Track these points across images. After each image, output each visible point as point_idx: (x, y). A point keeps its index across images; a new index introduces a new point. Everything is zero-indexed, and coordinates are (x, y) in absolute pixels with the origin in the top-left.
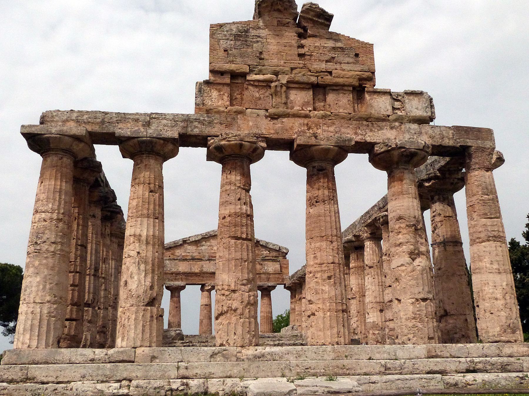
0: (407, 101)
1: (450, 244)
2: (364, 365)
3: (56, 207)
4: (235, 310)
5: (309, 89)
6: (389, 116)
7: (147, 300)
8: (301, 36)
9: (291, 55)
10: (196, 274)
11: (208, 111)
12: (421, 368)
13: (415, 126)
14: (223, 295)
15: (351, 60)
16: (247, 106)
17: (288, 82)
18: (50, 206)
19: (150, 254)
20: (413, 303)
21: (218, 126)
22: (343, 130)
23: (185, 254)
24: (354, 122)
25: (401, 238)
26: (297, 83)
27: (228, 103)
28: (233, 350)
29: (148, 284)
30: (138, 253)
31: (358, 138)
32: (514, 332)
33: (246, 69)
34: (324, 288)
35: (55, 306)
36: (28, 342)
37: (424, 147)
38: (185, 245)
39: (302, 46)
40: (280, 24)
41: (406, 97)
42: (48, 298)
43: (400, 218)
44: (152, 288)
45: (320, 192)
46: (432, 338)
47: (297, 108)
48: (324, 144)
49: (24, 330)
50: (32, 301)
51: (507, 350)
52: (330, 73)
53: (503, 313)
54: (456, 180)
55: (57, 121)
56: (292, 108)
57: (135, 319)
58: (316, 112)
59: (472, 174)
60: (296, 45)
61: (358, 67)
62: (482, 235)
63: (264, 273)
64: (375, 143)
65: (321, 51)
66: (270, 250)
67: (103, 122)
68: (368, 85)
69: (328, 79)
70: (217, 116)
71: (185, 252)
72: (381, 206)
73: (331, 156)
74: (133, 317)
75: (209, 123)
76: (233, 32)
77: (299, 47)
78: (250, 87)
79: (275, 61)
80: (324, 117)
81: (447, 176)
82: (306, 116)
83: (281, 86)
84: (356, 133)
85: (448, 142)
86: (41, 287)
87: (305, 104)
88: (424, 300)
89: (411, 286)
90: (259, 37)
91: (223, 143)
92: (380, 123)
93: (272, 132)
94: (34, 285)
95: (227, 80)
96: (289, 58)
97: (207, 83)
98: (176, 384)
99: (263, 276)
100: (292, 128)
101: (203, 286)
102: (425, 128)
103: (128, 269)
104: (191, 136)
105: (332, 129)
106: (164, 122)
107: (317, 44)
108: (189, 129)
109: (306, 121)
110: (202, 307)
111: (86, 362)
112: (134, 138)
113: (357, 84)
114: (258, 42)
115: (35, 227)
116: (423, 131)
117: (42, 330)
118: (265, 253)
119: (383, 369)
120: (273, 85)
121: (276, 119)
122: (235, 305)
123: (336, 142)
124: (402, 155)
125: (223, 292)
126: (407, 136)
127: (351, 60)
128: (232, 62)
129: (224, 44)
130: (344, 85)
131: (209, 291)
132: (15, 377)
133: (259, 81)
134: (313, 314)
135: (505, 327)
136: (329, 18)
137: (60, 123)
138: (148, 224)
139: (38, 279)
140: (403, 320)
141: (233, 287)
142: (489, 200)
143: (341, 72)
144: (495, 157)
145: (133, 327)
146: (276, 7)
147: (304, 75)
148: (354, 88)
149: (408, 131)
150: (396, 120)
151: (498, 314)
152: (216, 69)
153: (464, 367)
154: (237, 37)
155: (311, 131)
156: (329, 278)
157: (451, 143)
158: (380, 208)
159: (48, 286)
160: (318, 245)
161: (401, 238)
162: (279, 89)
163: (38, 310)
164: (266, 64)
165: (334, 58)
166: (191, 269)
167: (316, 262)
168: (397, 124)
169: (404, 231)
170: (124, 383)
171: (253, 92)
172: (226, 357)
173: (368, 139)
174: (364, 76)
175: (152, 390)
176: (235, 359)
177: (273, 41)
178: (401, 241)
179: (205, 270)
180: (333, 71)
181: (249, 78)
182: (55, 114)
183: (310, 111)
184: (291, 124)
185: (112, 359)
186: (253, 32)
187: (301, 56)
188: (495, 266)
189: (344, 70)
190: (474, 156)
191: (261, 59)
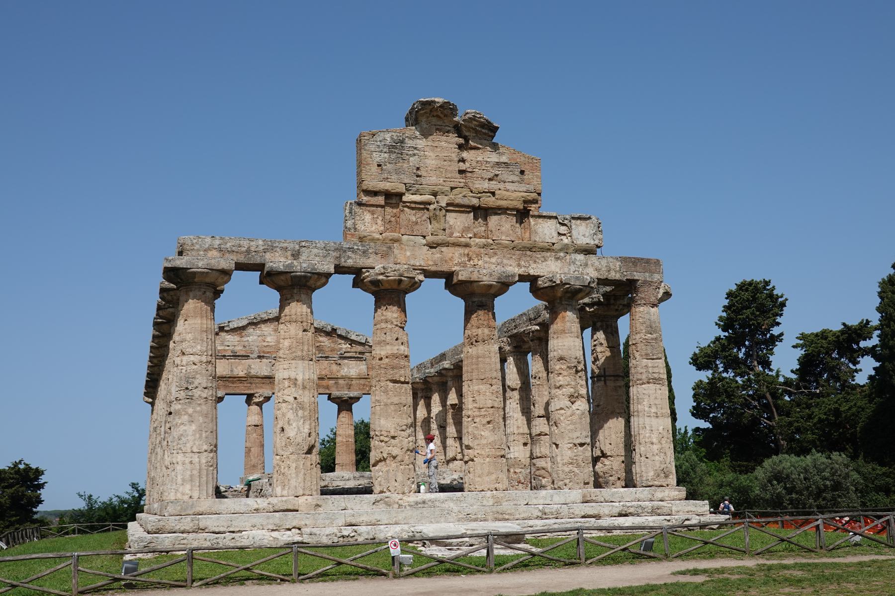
0: (573, 227)
1: (612, 378)
2: (523, 511)
3: (205, 349)
4: (394, 458)
5: (469, 212)
6: (553, 244)
7: (306, 448)
8: (461, 147)
9: (451, 172)
10: (239, 379)
11: (361, 239)
12: (576, 513)
13: (580, 257)
14: (382, 441)
15: (516, 178)
16: (403, 231)
17: (448, 205)
18: (199, 347)
19: (306, 400)
20: (570, 448)
21: (373, 256)
22: (505, 261)
23: (222, 348)
24: (518, 252)
25: (561, 380)
26: (458, 205)
27: (382, 228)
28: (395, 497)
29: (307, 431)
30: (295, 398)
31: (521, 271)
32: (666, 477)
33: (401, 188)
34: (483, 433)
35: (211, 455)
36: (188, 492)
37: (589, 283)
38: (223, 334)
39: (463, 160)
41: (573, 221)
42: (205, 447)
43: (561, 359)
45: (480, 331)
46: (588, 483)
47: (456, 234)
48: (486, 280)
49: (183, 480)
50: (189, 451)
51: (659, 494)
52: (493, 194)
53: (657, 458)
54: (621, 307)
55: (198, 250)
56: (451, 235)
57: (296, 468)
58: (477, 240)
59: (637, 310)
60: (456, 159)
61: (523, 188)
62: (644, 377)
63: (343, 378)
64: (539, 277)
65: (483, 167)
66: (352, 342)
67: (248, 251)
68: (533, 207)
69: (490, 201)
70: (372, 244)
71: (222, 344)
72: (532, 316)
73: (492, 291)
74: (294, 465)
75: (364, 252)
76: (388, 143)
77: (459, 161)
78: (406, 209)
79: (433, 179)
80: (484, 246)
81: (612, 301)
82: (467, 245)
83: (440, 210)
84: (519, 265)
85: (614, 276)
86: (198, 435)
87: (467, 229)
88: (582, 445)
89: (571, 431)
90: (416, 148)
91: (381, 277)
92: (544, 254)
93: (431, 263)
94: (191, 433)
95: (381, 200)
96: (449, 175)
98: (347, 531)
99: (341, 382)
100: (451, 259)
101: (249, 398)
103: (284, 415)
104: (343, 267)
105: (493, 260)
106: (315, 251)
107: (479, 159)
108: (343, 260)
109: (466, 251)
110: (249, 428)
111: (251, 512)
112: (287, 272)
113: (522, 207)
114: (414, 155)
115: (184, 371)
116: (589, 263)
117: (202, 480)
118: (345, 346)
119: (540, 514)
120: (432, 207)
121: (435, 248)
122: (395, 451)
123: (499, 278)
124: (567, 291)
125: (382, 438)
127: (516, 178)
129: (377, 157)
130: (508, 209)
131: (260, 404)
132: (187, 528)
133: (415, 203)
134: (472, 460)
135: (659, 471)
136: (495, 129)
137: (202, 253)
138: (304, 367)
139: (194, 427)
140: (560, 465)
141: (392, 434)
142: (652, 339)
143: (505, 193)
144: (661, 291)
145: (294, 475)
146: (435, 114)
147: (465, 196)
148: (518, 210)
149: (574, 263)
150: (561, 250)
151: (653, 458)
152: (370, 189)
153: (616, 511)
154: (391, 148)
155: (471, 262)
156: (489, 423)
157: (618, 276)
158: (530, 320)
159: (204, 435)
160: (476, 388)
161: (561, 380)
162: (438, 212)
163: (197, 460)
164: (424, 183)
165: (497, 175)
166: (232, 371)
167: (475, 405)
168: (562, 254)
169: (565, 373)
170: (293, 530)
171: (410, 215)
172: (388, 504)
173: (532, 272)
174: (529, 198)
175: (324, 537)
176: (397, 506)
177: (431, 154)
178: (561, 383)
179: (253, 372)
180: (497, 192)
181: (405, 198)
182: (195, 241)
183: (470, 238)
184: (451, 255)
185: (276, 508)
186: (409, 143)
187: (461, 172)
188: (654, 410)
189: (508, 191)
190: (641, 289)
191: (418, 176)
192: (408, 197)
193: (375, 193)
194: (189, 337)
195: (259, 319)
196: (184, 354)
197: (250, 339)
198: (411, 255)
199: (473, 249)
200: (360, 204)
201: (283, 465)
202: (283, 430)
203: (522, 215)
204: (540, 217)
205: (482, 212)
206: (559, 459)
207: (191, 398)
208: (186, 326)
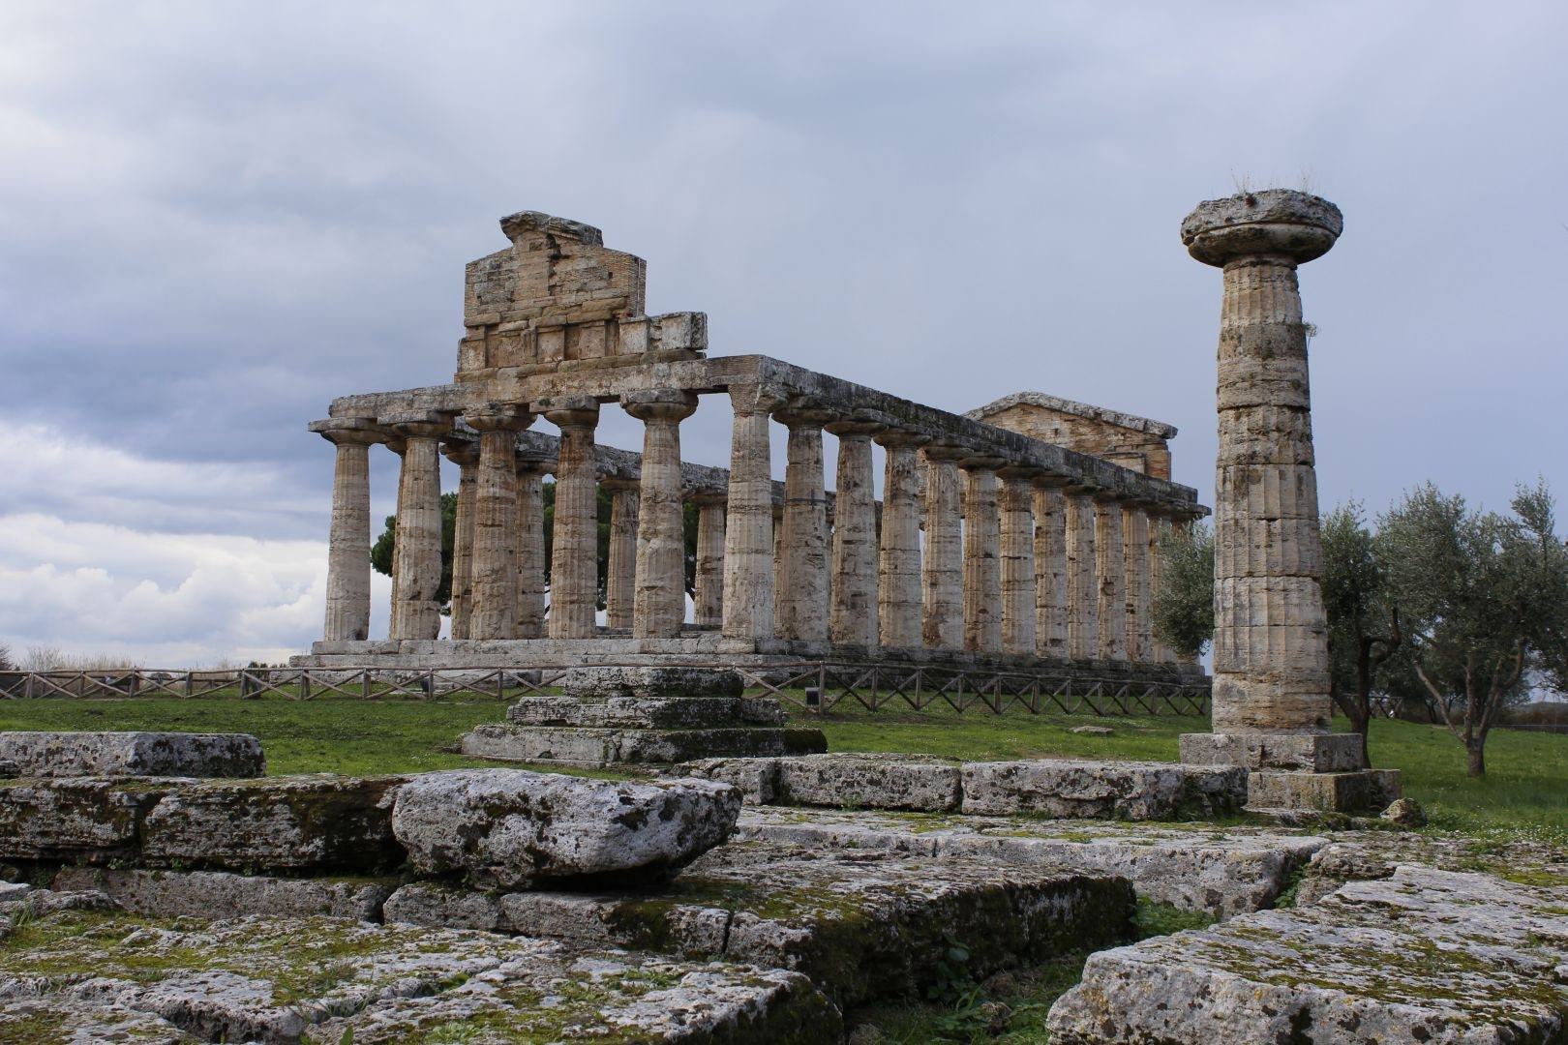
8: (556, 258)
13: (663, 366)
15: (603, 284)
31: (601, 392)
32: (740, 624)
33: (496, 318)
40: (535, 248)
44: (415, 581)
61: (609, 293)
69: (574, 317)
79: (524, 303)
80: (570, 368)
82: (552, 371)
97: (464, 341)
102: (677, 367)
109: (550, 377)
122: (479, 597)
126: (654, 381)
128: (485, 311)
148: (608, 322)
171: (508, 346)
181: (501, 328)
186: (506, 266)
193: (477, 327)
198: (508, 390)
199: (561, 374)
203: (612, 322)
205: (568, 329)
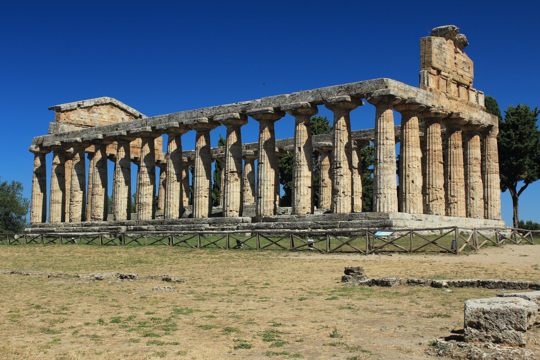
33: (440, 68)
38: (79, 110)
62: (494, 170)
71: (78, 117)
82: (457, 100)
91: (441, 112)
120: (449, 79)
134: (456, 203)
171: (442, 82)
186: (443, 46)
192: (442, 73)
194: (390, 131)
195: (100, 103)
196: (387, 139)
197: (94, 115)
200: (430, 73)
201: (414, 199)
202: (413, 182)
204: (472, 90)
206: (475, 205)
207: (392, 162)
208: (388, 125)
